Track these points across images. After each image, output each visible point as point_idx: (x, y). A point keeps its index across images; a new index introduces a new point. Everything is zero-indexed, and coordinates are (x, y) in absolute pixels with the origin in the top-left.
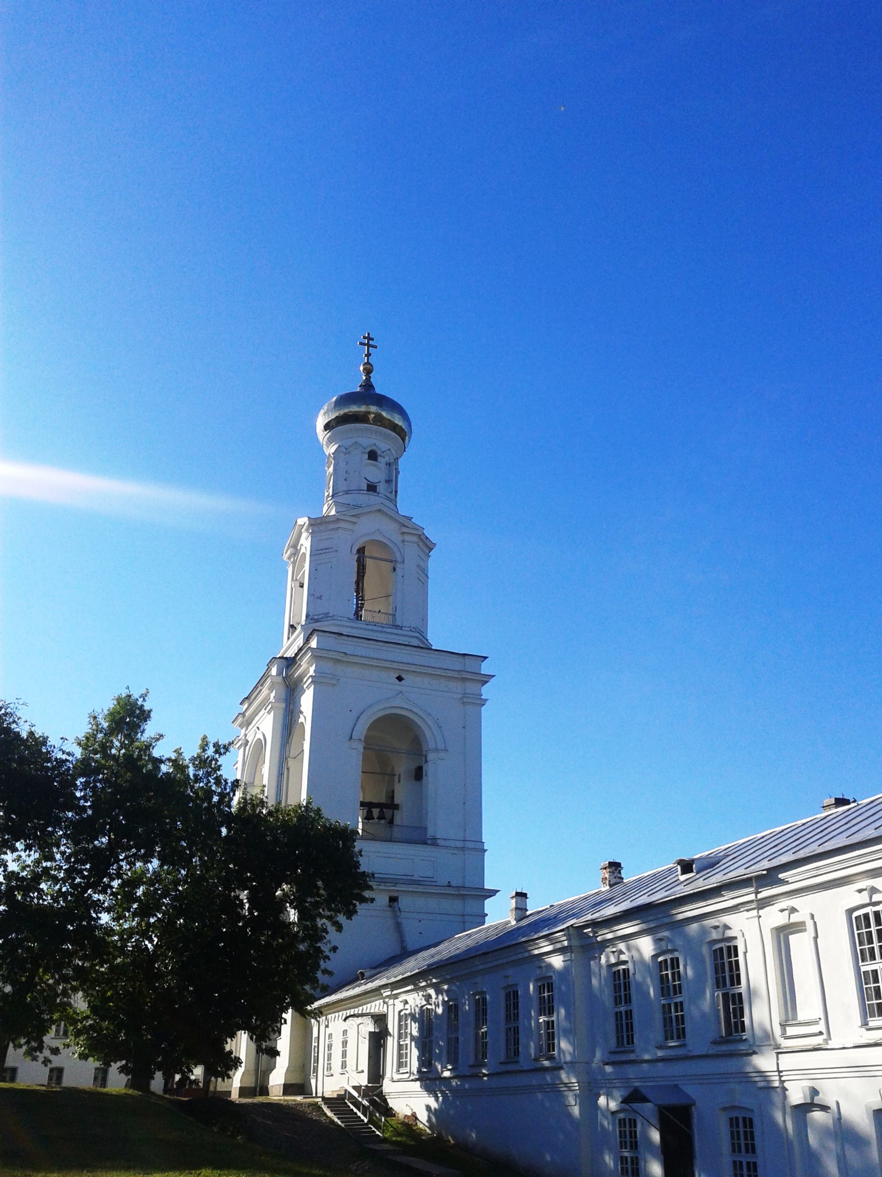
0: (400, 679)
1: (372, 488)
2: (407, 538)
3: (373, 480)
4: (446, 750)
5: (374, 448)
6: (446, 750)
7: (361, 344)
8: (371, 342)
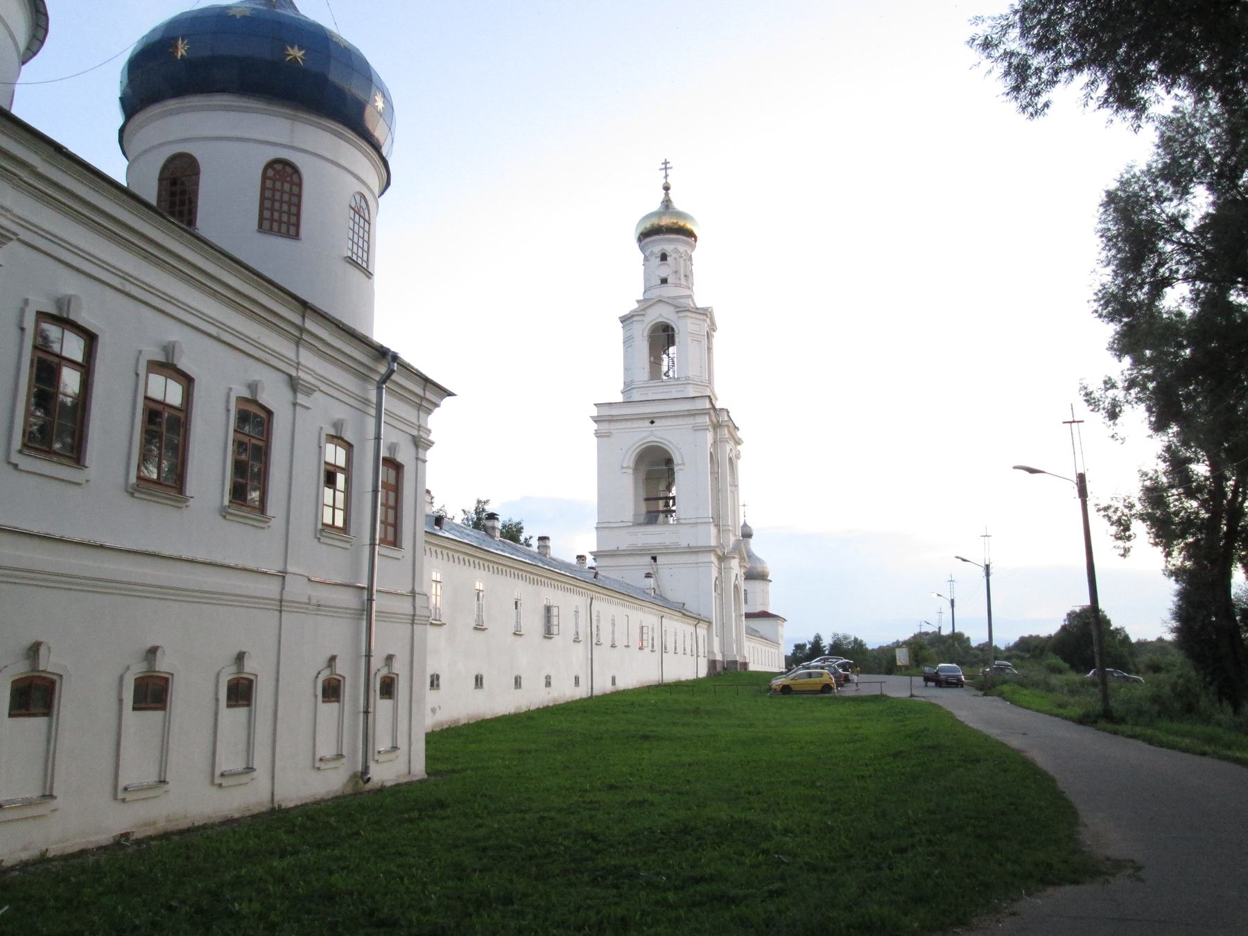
0: (652, 422)
1: (664, 281)
2: (681, 314)
3: (664, 275)
4: (683, 464)
5: (663, 251)
6: (683, 464)
7: (661, 169)
8: (668, 166)
